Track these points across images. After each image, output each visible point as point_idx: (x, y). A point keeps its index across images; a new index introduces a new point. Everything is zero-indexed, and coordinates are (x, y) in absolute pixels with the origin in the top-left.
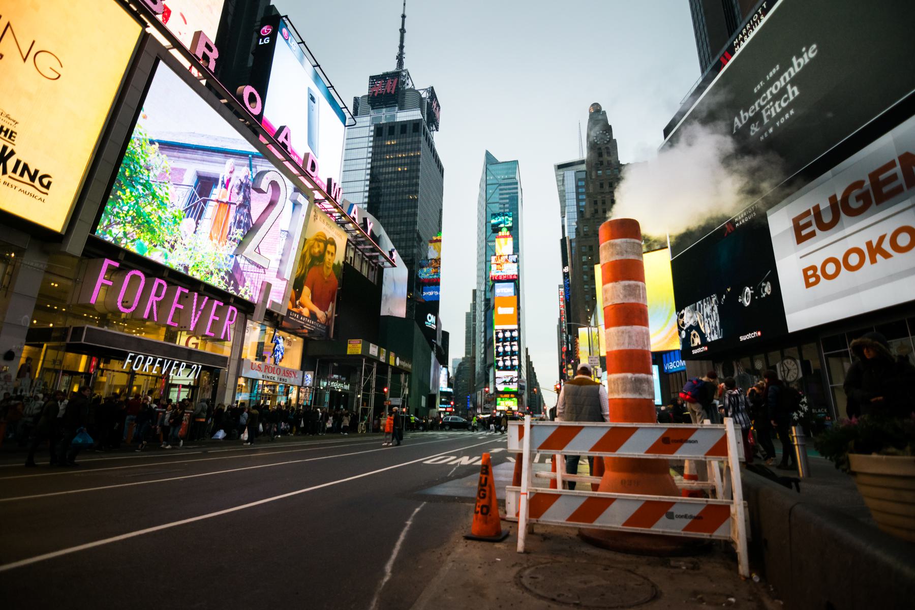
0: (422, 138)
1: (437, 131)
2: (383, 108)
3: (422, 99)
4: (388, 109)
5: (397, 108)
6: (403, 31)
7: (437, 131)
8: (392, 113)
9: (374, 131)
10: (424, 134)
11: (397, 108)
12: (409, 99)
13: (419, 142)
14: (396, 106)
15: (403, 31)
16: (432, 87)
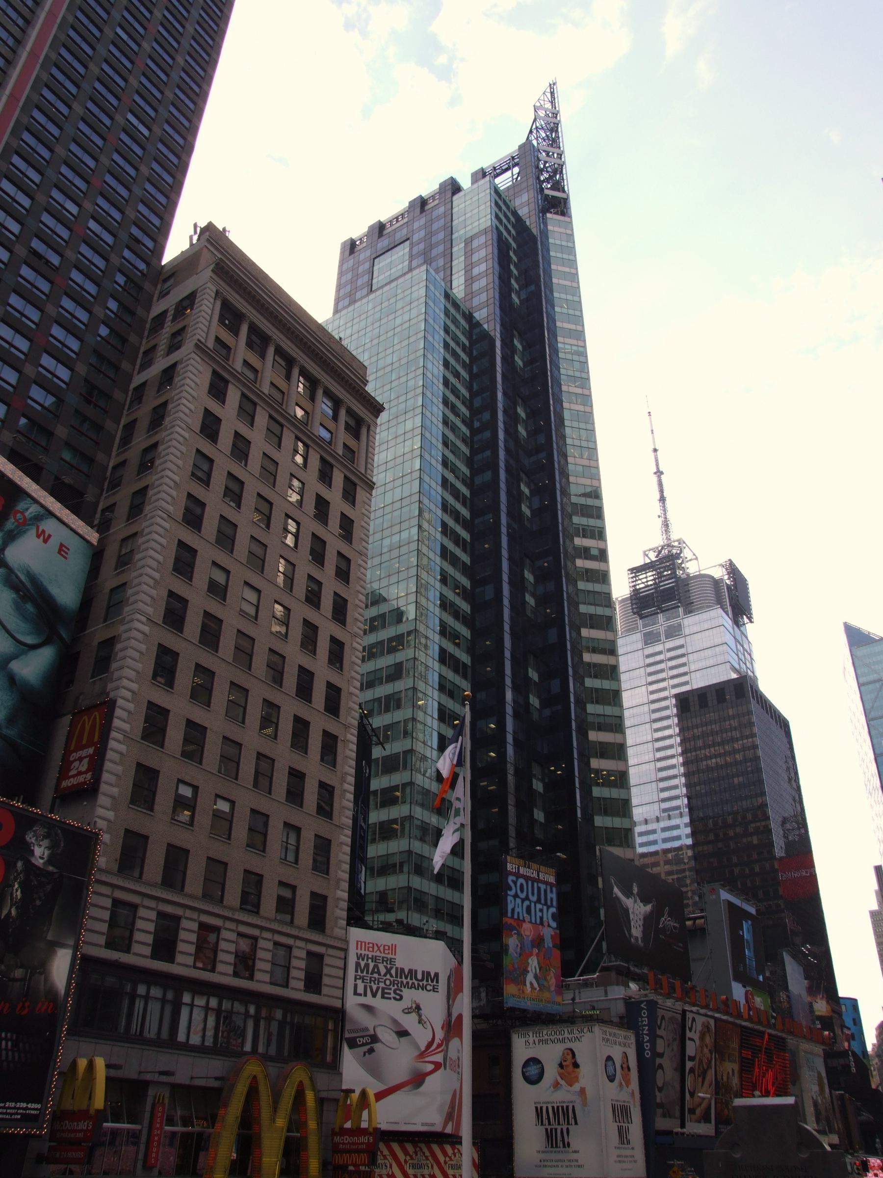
0: (753, 702)
1: (751, 622)
2: (658, 613)
3: (716, 583)
4: (668, 614)
5: (681, 610)
6: (659, 473)
7: (751, 622)
8: (673, 622)
9: (676, 706)
10: (753, 697)
11: (681, 610)
12: (695, 593)
13: (750, 713)
14: (679, 607)
15: (659, 473)
16: (731, 563)
